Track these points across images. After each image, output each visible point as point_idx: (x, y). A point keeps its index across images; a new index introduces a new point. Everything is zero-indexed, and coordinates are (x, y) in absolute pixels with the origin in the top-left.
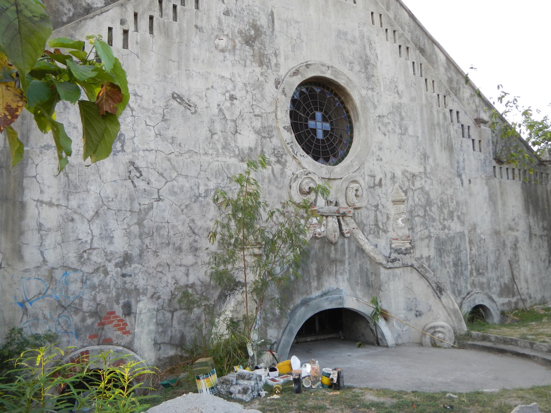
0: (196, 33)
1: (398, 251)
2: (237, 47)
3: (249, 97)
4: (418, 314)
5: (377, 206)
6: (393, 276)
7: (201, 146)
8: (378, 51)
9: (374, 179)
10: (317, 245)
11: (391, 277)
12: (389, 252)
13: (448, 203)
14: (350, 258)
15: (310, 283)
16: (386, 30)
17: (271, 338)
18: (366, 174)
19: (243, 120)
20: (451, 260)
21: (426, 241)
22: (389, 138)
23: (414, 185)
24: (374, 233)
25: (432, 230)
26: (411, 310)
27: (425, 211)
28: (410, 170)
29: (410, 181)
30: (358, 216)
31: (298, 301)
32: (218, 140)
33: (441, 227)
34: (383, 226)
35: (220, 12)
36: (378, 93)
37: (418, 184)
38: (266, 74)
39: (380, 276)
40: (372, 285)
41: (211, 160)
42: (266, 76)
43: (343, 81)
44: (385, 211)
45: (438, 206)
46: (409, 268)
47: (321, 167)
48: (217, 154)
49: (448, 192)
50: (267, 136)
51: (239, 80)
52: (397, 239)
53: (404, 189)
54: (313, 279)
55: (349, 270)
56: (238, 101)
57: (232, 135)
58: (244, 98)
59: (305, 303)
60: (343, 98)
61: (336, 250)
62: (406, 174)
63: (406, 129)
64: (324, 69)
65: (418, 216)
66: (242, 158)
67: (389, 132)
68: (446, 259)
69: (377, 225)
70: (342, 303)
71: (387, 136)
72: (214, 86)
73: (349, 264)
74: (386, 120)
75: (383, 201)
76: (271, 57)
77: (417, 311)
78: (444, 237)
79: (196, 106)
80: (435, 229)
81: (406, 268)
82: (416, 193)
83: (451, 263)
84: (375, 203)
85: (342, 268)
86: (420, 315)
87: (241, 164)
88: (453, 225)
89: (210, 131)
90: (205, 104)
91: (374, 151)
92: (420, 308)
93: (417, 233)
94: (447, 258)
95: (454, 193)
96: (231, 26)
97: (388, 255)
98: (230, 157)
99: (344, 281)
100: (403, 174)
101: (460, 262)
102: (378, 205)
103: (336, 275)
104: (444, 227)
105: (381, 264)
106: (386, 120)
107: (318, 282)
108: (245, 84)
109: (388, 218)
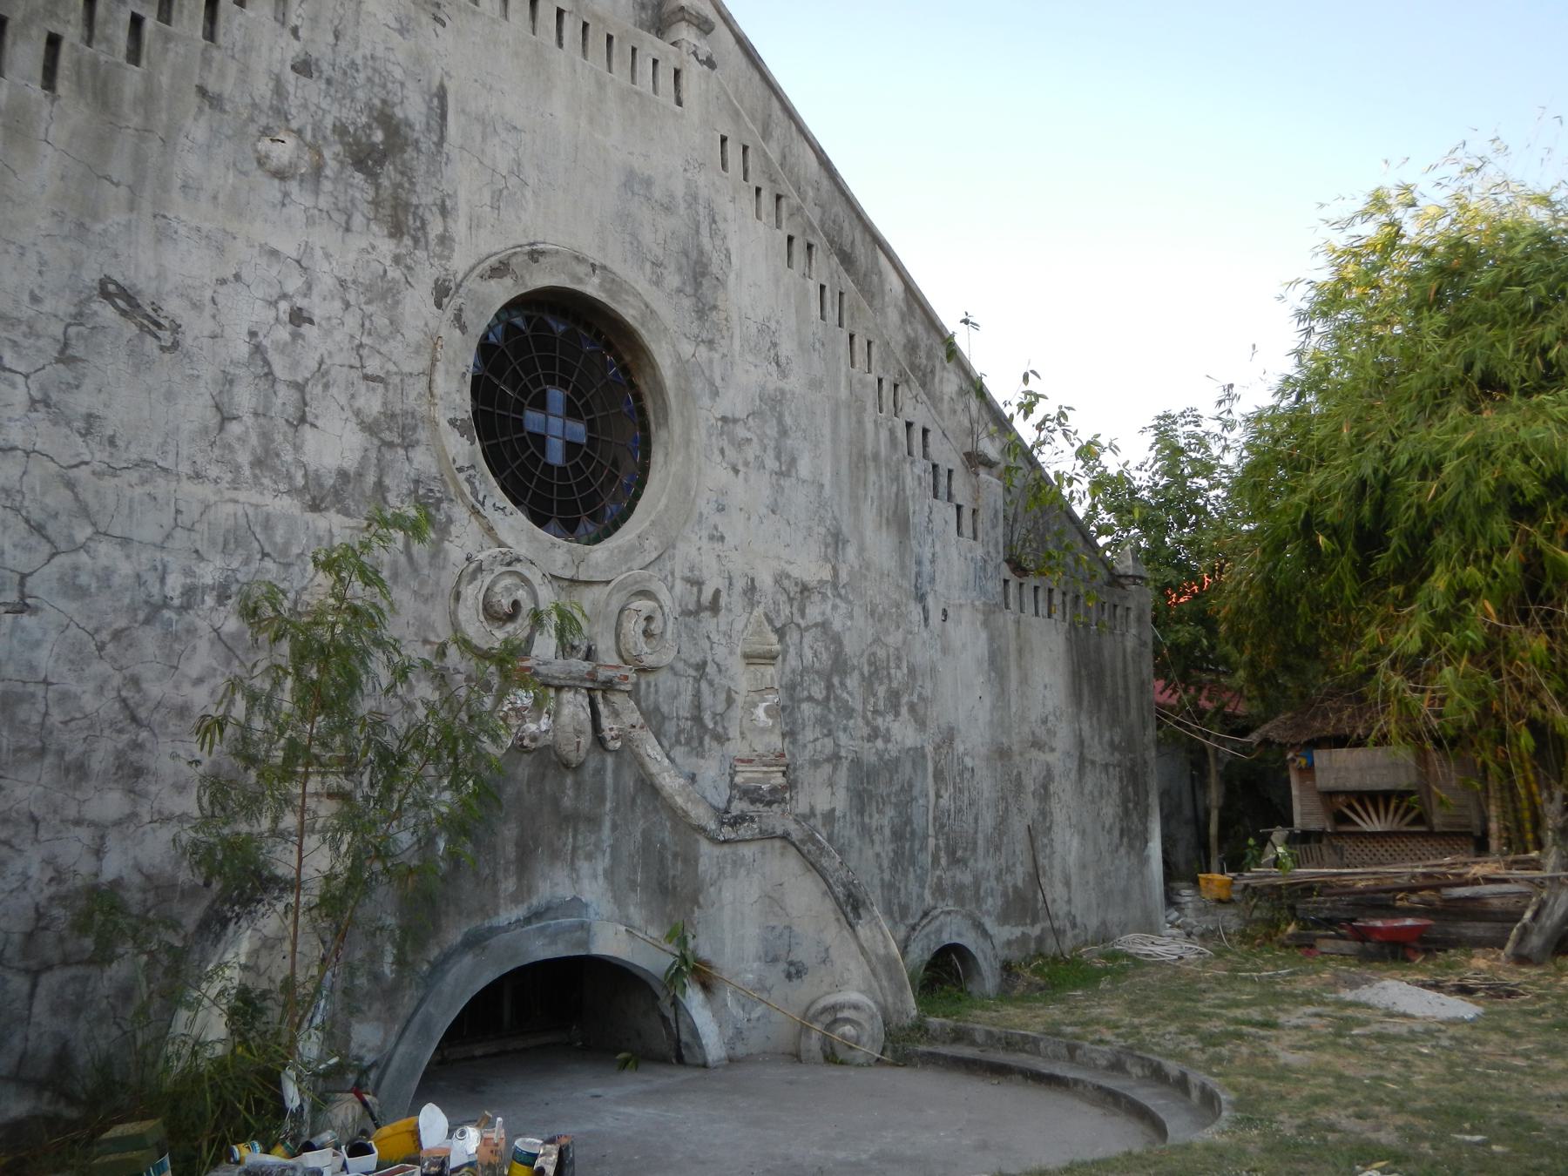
0: (200, 110)
1: (751, 794)
2: (328, 172)
3: (352, 321)
4: (793, 970)
5: (701, 667)
6: (734, 862)
7: (184, 452)
8: (733, 244)
9: (700, 591)
10: (523, 771)
11: (729, 867)
13: (888, 668)
14: (616, 810)
15: (496, 882)
16: (758, 190)
17: (363, 1052)
19: (326, 386)
20: (886, 822)
21: (827, 769)
22: (746, 480)
23: (803, 615)
24: (688, 743)
25: (843, 739)
26: (775, 960)
27: (830, 687)
28: (795, 572)
29: (796, 604)
30: (648, 693)
31: (454, 936)
32: (242, 440)
33: (866, 731)
34: (716, 723)
35: (283, 61)
36: (724, 356)
37: (814, 612)
38: (409, 261)
39: (696, 861)
40: (675, 888)
41: (213, 499)
42: (409, 268)
43: (632, 312)
44: (724, 682)
45: (862, 674)
46: (778, 844)
47: (553, 544)
48: (233, 481)
49: (890, 640)
50: (397, 440)
51: (326, 267)
52: (750, 761)
53: (778, 625)
54: (506, 870)
55: (613, 847)
56: (315, 328)
57: (286, 428)
58: (335, 321)
59: (475, 941)
60: (628, 358)
61: (578, 785)
62: (786, 583)
63: (793, 461)
64: (582, 270)
65: (810, 699)
66: (314, 499)
67: (746, 464)
68: (875, 820)
69: (697, 719)
70: (585, 943)
72: (244, 275)
73: (614, 827)
74: (741, 432)
75: (721, 652)
76: (428, 216)
77: (791, 964)
78: (874, 759)
79: (176, 328)
80: (852, 738)
81: (768, 843)
83: (887, 832)
84: (698, 659)
85: (593, 838)
86: (799, 974)
87: (309, 516)
88: (896, 728)
89: (217, 407)
90: (209, 326)
91: (705, 513)
92: (799, 955)
93: (805, 746)
94: (876, 816)
95: (904, 642)
96: (313, 108)
97: (722, 805)
98: (277, 493)
99: (595, 877)
100: (776, 582)
102: (705, 663)
103: (572, 862)
104: (874, 734)
105: (702, 829)
106: (741, 432)
107: (520, 879)
108: (342, 283)
109: (730, 701)
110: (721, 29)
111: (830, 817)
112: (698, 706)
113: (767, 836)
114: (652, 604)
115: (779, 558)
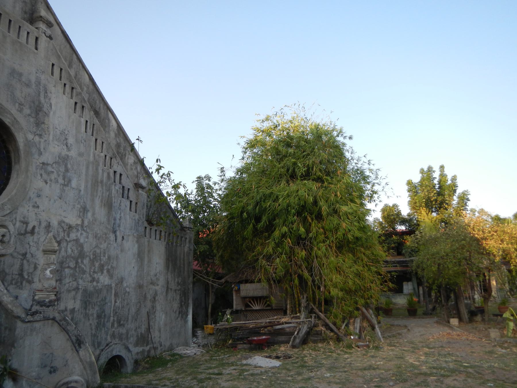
1: (41, 303)
4: (52, 370)
5: (25, 255)
8: (53, 102)
9: (27, 226)
12: (30, 304)
13: (100, 256)
16: (65, 85)
18: (18, 219)
22: (50, 186)
23: (69, 236)
24: (16, 284)
25: (81, 282)
26: (45, 366)
27: (77, 263)
28: (67, 220)
29: (66, 232)
33: (90, 279)
34: (29, 276)
36: (46, 141)
37: (73, 236)
39: (15, 331)
43: (8, 120)
44: (34, 260)
45: (90, 258)
46: (50, 321)
49: (102, 246)
52: (42, 291)
53: (58, 240)
62: (63, 224)
63: (70, 181)
67: (51, 180)
69: (21, 275)
71: (48, 184)
74: (50, 169)
75: (33, 249)
77: (52, 367)
80: (84, 282)
81: (46, 322)
82: (70, 245)
83: (95, 316)
84: (24, 252)
86: (55, 371)
88: (101, 278)
93: (65, 285)
94: (91, 310)
95: (107, 247)
97: (28, 307)
101: (103, 314)
102: (26, 254)
105: (18, 317)
109: (35, 268)
110: (56, 26)
111: (73, 311)
112: (22, 270)
113: (46, 319)
114: (5, 230)
115: (61, 215)
